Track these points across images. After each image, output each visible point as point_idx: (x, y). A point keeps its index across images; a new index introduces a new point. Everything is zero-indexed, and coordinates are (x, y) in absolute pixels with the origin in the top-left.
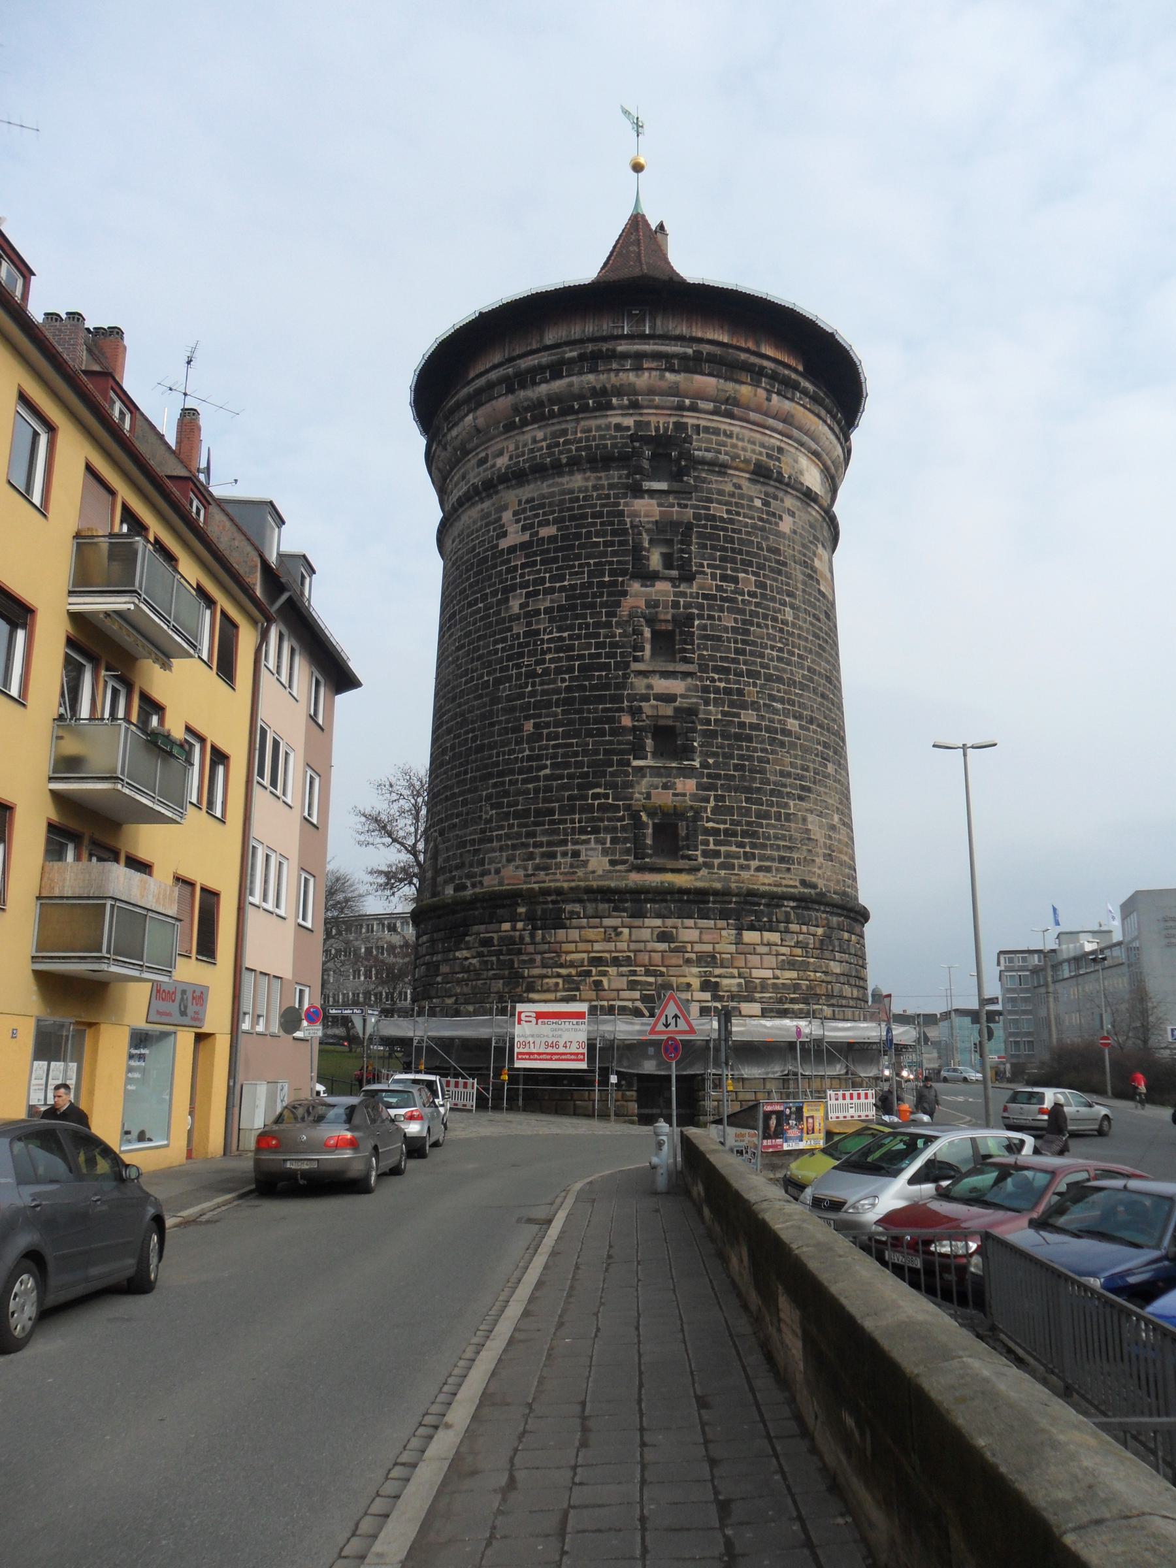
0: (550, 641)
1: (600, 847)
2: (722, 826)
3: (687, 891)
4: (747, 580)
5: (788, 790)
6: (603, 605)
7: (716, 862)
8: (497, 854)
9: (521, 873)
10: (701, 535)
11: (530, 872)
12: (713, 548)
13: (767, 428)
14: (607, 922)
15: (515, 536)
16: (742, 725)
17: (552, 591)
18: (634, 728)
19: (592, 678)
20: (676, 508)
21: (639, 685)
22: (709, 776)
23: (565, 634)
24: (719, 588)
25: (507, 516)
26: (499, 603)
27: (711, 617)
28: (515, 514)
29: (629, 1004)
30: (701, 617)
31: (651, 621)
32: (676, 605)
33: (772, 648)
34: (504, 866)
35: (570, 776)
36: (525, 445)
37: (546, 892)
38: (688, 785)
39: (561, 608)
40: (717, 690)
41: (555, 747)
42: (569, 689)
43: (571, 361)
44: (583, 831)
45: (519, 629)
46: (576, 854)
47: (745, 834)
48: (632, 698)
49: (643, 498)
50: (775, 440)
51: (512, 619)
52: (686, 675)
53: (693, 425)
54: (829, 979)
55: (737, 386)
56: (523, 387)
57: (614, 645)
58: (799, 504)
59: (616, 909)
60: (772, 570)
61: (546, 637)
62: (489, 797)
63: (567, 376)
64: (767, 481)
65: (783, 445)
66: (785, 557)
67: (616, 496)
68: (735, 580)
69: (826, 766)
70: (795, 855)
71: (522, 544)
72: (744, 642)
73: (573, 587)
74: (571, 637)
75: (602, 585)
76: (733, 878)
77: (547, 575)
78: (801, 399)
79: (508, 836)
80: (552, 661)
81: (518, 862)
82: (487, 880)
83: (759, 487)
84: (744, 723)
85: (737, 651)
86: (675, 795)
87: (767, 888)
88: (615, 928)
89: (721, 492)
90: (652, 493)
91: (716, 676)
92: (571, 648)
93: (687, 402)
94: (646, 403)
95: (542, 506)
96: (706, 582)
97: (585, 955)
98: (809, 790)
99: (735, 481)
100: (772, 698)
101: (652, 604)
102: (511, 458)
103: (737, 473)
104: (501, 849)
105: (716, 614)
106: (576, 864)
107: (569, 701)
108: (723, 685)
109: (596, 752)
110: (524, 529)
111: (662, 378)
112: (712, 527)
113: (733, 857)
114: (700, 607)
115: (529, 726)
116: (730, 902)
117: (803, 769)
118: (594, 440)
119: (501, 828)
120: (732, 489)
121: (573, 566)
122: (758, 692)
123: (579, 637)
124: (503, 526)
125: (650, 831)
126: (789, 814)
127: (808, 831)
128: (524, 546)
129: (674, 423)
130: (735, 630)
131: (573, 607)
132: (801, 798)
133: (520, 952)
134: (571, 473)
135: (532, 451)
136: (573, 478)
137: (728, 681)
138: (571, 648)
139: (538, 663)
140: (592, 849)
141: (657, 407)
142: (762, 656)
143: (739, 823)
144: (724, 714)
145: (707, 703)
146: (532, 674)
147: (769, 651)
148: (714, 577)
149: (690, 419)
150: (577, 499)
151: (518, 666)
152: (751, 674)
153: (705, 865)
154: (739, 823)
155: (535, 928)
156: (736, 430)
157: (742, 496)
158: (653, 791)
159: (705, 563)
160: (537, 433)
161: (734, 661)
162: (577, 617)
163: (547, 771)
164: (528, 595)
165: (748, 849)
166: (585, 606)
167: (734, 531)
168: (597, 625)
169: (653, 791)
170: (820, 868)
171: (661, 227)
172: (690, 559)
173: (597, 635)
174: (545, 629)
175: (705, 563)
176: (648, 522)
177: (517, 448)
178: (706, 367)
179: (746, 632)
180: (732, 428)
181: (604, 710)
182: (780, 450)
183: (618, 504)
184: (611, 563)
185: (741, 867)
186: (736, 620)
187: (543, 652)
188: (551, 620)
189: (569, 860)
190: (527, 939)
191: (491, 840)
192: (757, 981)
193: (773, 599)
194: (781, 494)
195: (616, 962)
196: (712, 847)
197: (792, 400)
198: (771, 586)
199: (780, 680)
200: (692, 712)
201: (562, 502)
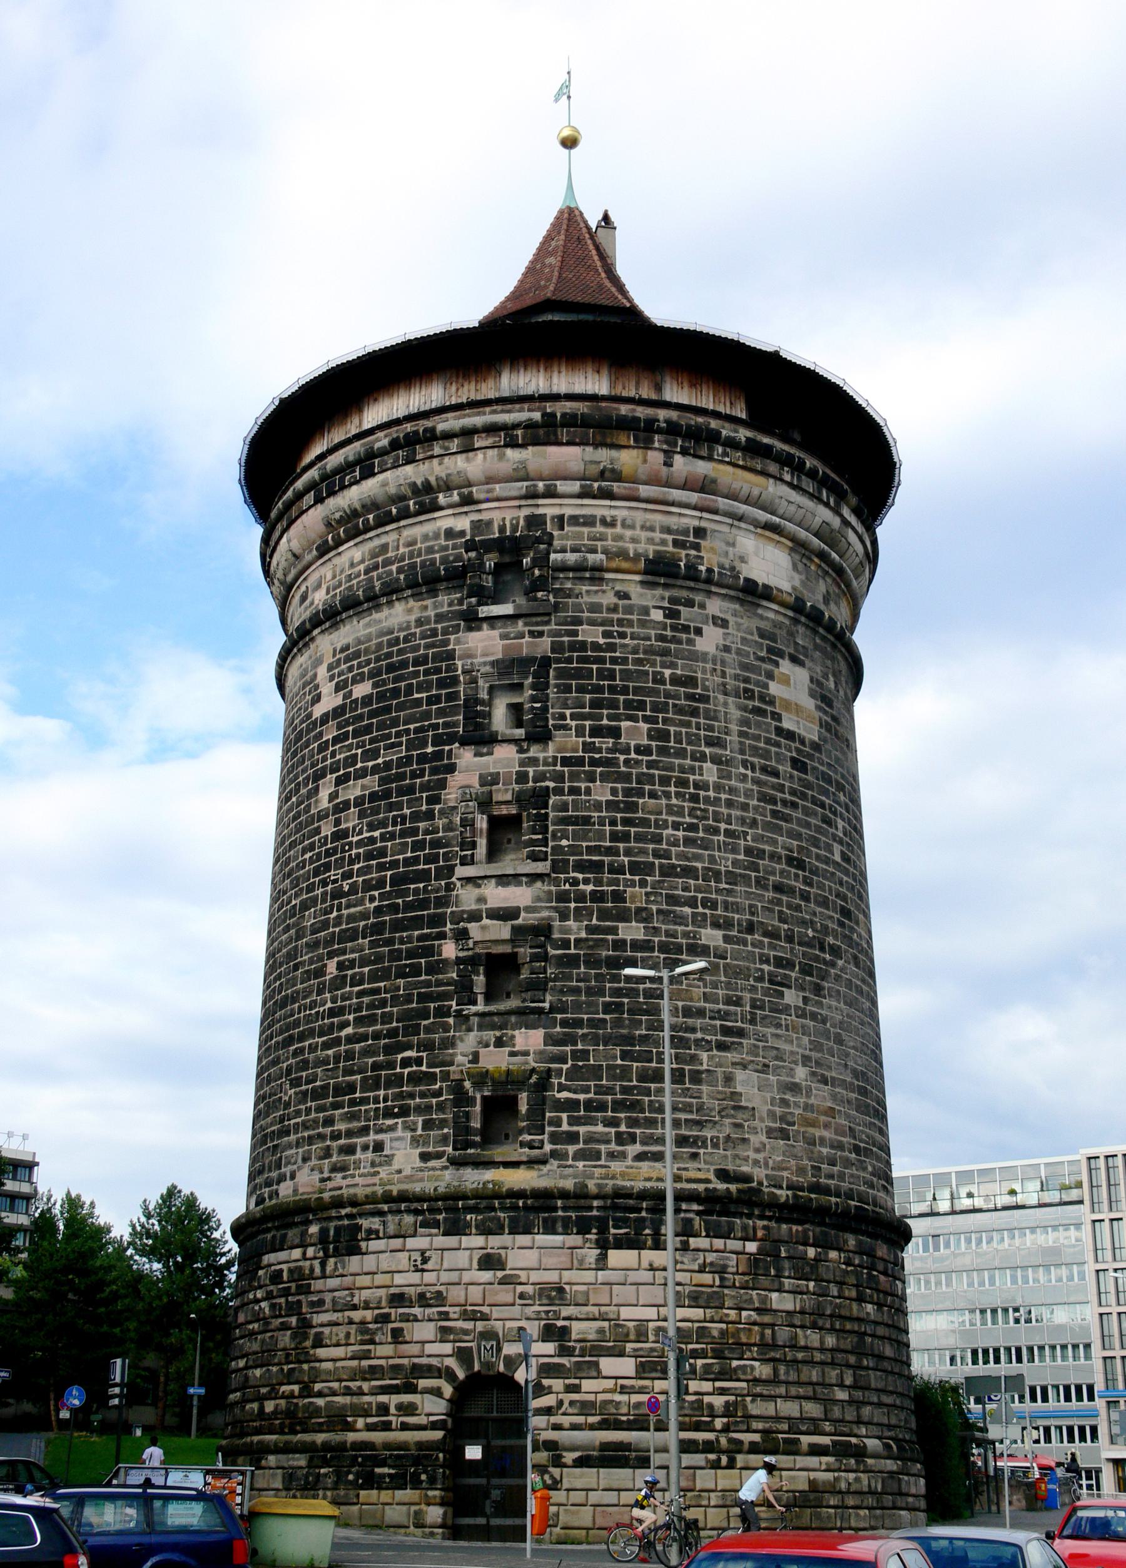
0: (360, 844)
1: (409, 1134)
2: (581, 1097)
3: (520, 1194)
4: (636, 732)
5: (699, 1035)
6: (424, 787)
7: (571, 1149)
8: (293, 1151)
9: (317, 1176)
10: (561, 674)
11: (326, 1175)
12: (581, 689)
13: (673, 504)
14: (411, 1243)
15: (329, 701)
16: (619, 945)
17: (362, 774)
18: (459, 961)
19: (404, 894)
20: (527, 639)
21: (467, 898)
22: (565, 1023)
23: (377, 834)
24: (588, 747)
27: (574, 791)
28: (330, 668)
29: (434, 1361)
30: (559, 791)
31: (485, 803)
32: (522, 777)
33: (676, 826)
34: (299, 1168)
35: (377, 1036)
36: (342, 572)
37: (338, 1203)
38: (530, 1039)
39: (373, 797)
40: (581, 897)
41: (360, 994)
42: (378, 911)
43: (383, 452)
44: (388, 1113)
45: (327, 830)
46: (379, 1147)
47: (618, 1106)
48: (457, 918)
49: (479, 629)
50: (690, 520)
52: (534, 877)
53: (553, 518)
54: (767, 1319)
55: (614, 453)
56: (332, 493)
57: (436, 844)
58: (737, 607)
59: (425, 1224)
60: (679, 710)
61: (355, 839)
62: (289, 1071)
63: (379, 473)
64: (670, 581)
65: (704, 524)
66: (705, 688)
67: (445, 632)
68: (615, 733)
69: (781, 995)
70: (708, 1133)
71: (335, 710)
72: (626, 822)
73: (388, 765)
74: (383, 838)
75: (423, 759)
76: (598, 1172)
77: (359, 751)
78: (725, 454)
79: (305, 1126)
80: (360, 872)
81: (314, 1162)
83: (659, 592)
84: (624, 941)
85: (615, 837)
86: (512, 1054)
87: (648, 1185)
88: (423, 1252)
89: (595, 608)
90: (492, 620)
91: (580, 876)
92: (382, 853)
93: (541, 485)
94: (482, 496)
95: (357, 655)
96: (568, 741)
97: (382, 1292)
98: (741, 1033)
99: (618, 588)
100: (672, 900)
101: (490, 780)
102: (328, 593)
103: (620, 576)
104: (298, 1145)
105: (583, 785)
106: (377, 1160)
107: (378, 928)
108: (590, 888)
109: (408, 999)
110: (338, 688)
111: (502, 457)
112: (581, 660)
113: (599, 1141)
114: (559, 778)
115: (332, 967)
116: (591, 1208)
117: (728, 1001)
118: (419, 555)
119: (298, 1113)
120: (615, 600)
121: (389, 736)
122: (647, 894)
123: (392, 836)
125: (478, 1108)
126: (699, 1072)
127: (735, 1096)
128: (338, 712)
129: (527, 518)
130: (612, 805)
131: (387, 794)
132: (722, 1047)
134: (390, 603)
135: (350, 578)
136: (392, 611)
137: (598, 882)
138: (382, 853)
139: (347, 875)
140: (398, 1139)
141: (498, 499)
142: (658, 839)
143: (609, 1091)
144: (590, 930)
145: (564, 917)
146: (338, 894)
147: (670, 831)
148: (580, 732)
149: (549, 509)
150: (397, 641)
151: (324, 883)
152: (635, 868)
153: (554, 1154)
154: (609, 1091)
155: (327, 1256)
156: (620, 514)
157: (629, 610)
158: (482, 1051)
159: (568, 712)
160: (353, 554)
161: (610, 851)
162: (391, 807)
163: (349, 1030)
164: (339, 782)
165: (623, 1128)
166: (401, 792)
167: (614, 661)
168: (416, 817)
169: (482, 1051)
170: (757, 1151)
171: (606, 218)
172: (545, 709)
173: (414, 832)
174: (354, 828)
175: (568, 712)
176: (485, 664)
178: (564, 434)
179: (632, 807)
180: (614, 512)
181: (421, 938)
182: (700, 532)
183: (446, 643)
184: (435, 727)
185: (612, 1156)
186: (614, 792)
187: (352, 862)
188: (361, 815)
189: (369, 1155)
190: (318, 1271)
191: (288, 1133)
192: (631, 1324)
193: (681, 753)
194: (698, 598)
195: (423, 1300)
196: (565, 1127)
197: (710, 458)
198: (678, 734)
199: (689, 872)
200: (542, 931)
201: (380, 646)
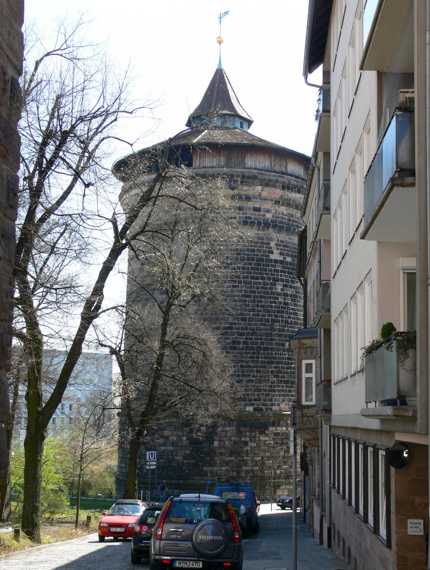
8: (278, 397)
25: (273, 244)
28: (276, 245)
36: (279, 214)
51: (278, 294)
61: (291, 307)
62: (272, 372)
79: (282, 391)
95: (286, 246)
102: (273, 217)
104: (279, 396)
119: (279, 386)
124: (271, 248)
128: (282, 262)
146: (287, 322)
160: (283, 209)
177: (276, 213)
191: (275, 391)
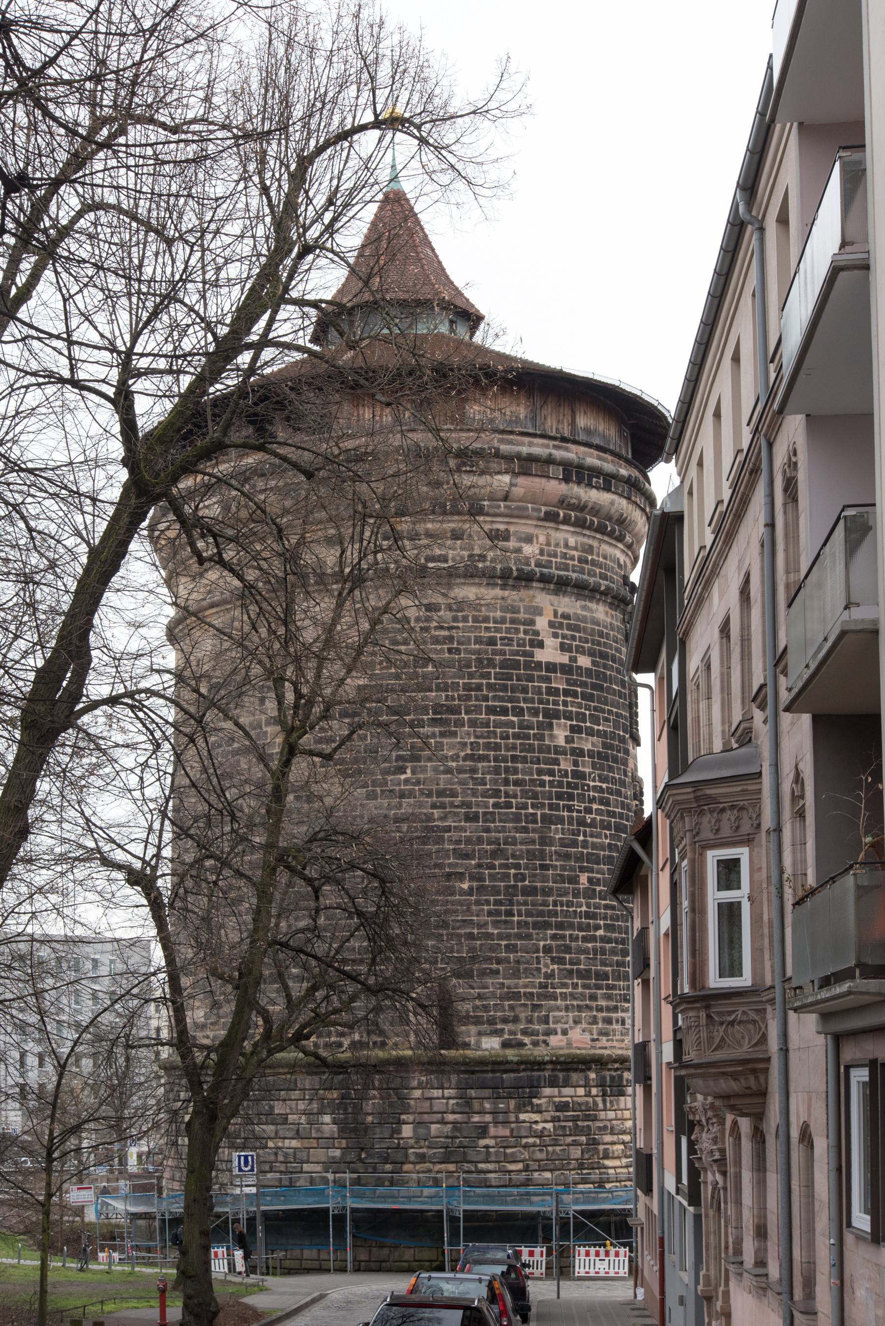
8: (563, 1013)
9: (587, 1037)
25: (541, 623)
26: (540, 725)
28: (551, 624)
34: (571, 1028)
36: (557, 545)
51: (558, 750)
61: (592, 784)
79: (573, 997)
82: (554, 1040)
95: (577, 628)
102: (542, 552)
104: (567, 1009)
115: (584, 878)
119: (565, 985)
124: (537, 633)
128: (566, 669)
133: (595, 1119)
146: (582, 822)
177: (548, 544)
